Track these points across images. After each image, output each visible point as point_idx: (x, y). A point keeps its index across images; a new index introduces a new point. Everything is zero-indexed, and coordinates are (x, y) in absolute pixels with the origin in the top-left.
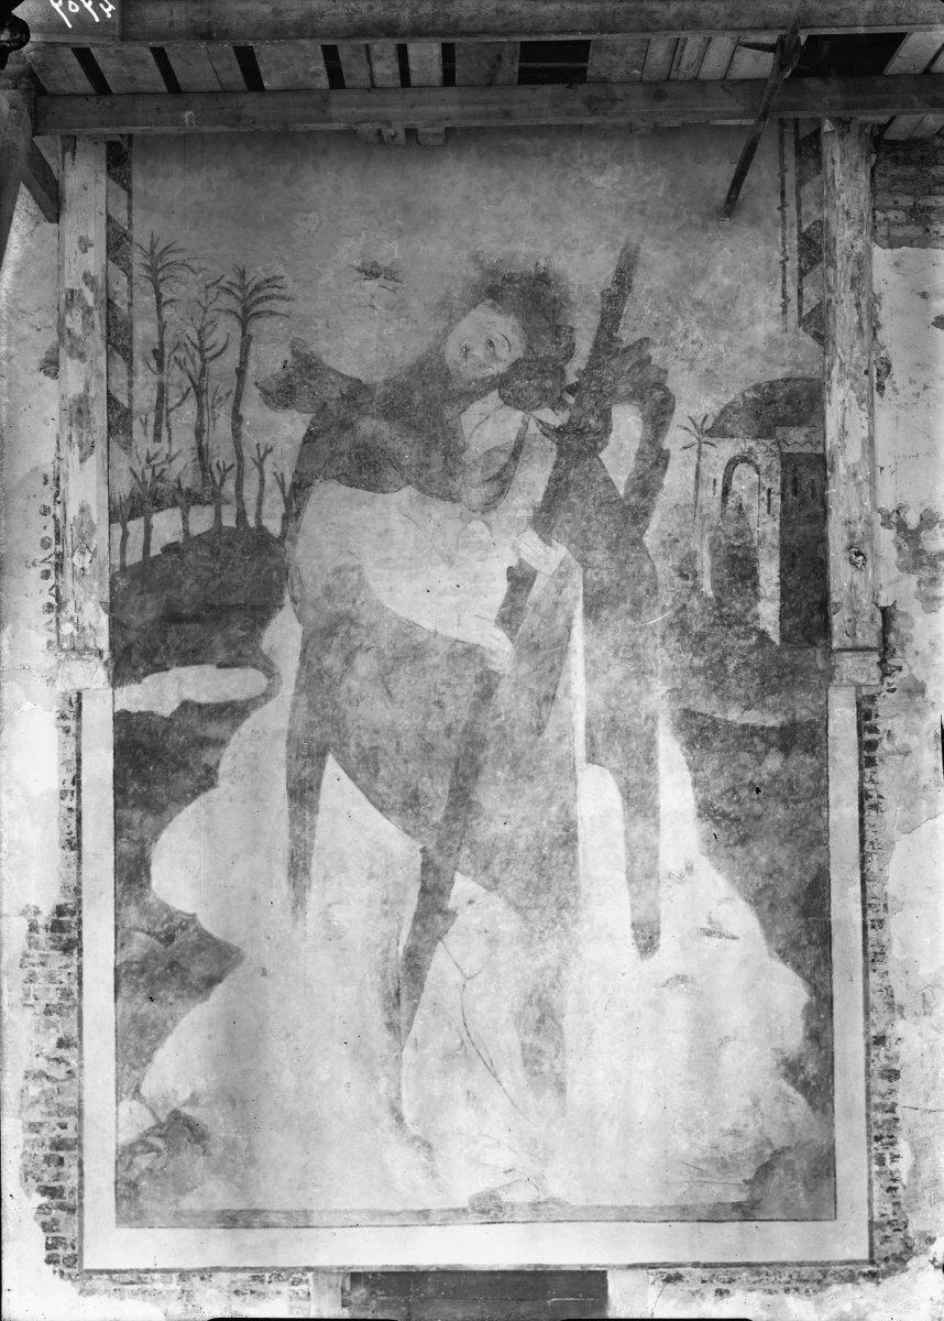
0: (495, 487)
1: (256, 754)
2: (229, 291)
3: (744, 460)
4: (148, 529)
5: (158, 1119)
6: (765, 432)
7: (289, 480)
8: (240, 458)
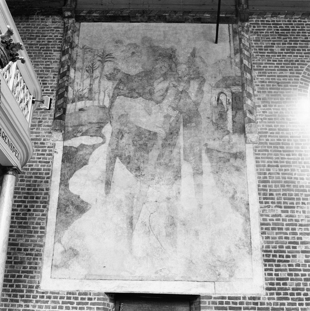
3: (222, 93)
4: (76, 105)
6: (227, 87)
7: (111, 95)
8: (100, 91)
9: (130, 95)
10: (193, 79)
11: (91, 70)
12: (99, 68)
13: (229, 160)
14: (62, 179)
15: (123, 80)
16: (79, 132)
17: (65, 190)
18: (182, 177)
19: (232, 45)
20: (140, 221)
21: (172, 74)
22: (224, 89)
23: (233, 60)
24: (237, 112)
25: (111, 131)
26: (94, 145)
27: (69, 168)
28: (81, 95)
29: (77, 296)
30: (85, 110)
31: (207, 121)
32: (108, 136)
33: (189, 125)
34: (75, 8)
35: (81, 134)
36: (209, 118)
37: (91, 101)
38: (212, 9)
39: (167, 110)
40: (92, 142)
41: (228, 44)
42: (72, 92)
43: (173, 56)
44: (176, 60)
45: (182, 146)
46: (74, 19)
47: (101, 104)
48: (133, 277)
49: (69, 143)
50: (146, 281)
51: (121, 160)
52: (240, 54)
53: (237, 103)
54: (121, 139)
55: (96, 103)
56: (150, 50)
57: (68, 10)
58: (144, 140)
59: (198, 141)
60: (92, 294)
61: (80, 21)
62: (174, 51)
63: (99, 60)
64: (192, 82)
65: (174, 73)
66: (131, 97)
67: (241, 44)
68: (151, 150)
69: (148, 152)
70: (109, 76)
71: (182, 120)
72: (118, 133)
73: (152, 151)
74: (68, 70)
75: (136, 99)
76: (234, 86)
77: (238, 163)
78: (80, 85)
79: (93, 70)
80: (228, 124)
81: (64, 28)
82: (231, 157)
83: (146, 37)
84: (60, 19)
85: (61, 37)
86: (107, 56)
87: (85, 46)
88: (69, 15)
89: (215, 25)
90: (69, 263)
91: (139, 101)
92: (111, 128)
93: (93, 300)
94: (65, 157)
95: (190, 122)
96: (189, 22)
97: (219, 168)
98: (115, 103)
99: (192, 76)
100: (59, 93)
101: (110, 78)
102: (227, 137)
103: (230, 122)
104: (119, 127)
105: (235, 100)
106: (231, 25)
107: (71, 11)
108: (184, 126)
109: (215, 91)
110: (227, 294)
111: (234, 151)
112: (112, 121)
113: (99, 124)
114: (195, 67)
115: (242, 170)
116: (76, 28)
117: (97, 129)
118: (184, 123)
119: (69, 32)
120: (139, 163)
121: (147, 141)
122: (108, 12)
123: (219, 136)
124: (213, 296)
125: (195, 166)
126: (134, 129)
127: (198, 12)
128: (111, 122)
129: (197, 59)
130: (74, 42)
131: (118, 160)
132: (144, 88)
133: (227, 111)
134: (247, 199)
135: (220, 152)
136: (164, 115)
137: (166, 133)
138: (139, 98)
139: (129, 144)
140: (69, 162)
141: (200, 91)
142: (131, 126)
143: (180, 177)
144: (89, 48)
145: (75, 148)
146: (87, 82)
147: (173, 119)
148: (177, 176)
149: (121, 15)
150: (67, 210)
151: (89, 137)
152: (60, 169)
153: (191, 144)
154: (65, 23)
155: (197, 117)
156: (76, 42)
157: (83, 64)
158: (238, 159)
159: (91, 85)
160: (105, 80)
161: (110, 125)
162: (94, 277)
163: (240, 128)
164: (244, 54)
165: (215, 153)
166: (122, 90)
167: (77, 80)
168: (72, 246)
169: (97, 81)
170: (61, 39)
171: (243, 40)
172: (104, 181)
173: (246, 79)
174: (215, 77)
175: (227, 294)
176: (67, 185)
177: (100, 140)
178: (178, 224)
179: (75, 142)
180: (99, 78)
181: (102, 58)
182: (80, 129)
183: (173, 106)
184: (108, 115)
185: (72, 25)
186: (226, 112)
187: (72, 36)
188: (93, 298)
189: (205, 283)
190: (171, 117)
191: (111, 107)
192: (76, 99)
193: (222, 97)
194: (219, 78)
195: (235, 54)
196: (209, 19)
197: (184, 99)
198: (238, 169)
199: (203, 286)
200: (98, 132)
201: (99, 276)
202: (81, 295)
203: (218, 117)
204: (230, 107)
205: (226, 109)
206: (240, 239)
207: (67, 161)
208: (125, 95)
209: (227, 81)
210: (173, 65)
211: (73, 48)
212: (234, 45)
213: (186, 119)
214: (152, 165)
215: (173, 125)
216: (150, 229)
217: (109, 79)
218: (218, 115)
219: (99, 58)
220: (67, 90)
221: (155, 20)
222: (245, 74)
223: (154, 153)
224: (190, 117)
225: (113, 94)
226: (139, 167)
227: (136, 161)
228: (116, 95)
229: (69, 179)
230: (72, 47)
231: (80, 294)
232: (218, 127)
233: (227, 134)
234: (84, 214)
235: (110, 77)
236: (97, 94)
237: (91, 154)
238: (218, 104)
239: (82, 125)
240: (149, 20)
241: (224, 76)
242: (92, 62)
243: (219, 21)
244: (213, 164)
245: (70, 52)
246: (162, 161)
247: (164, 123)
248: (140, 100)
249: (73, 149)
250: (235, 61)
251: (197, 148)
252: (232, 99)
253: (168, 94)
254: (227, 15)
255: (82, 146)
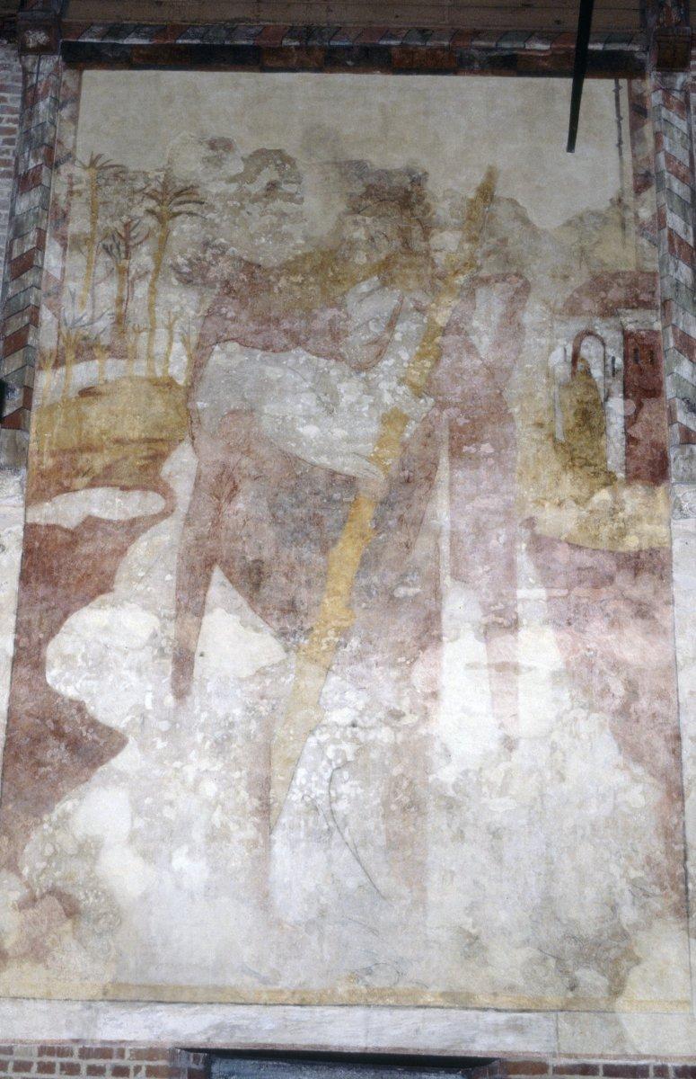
0: (374, 349)
1: (152, 562)
2: (151, 197)
3: (590, 333)
4: (67, 376)
5: (32, 892)
6: (608, 312)
7: (194, 339)
8: (153, 322)
9: (259, 340)
10: (485, 281)
11: (120, 245)
12: (151, 240)
13: (611, 579)
14: (21, 645)
15: (235, 285)
16: (80, 473)
17: (33, 683)
18: (444, 639)
19: (628, 156)
20: (296, 796)
21: (411, 265)
22: (598, 321)
23: (629, 215)
24: (640, 405)
25: (194, 472)
26: (133, 522)
27: (45, 604)
28: (85, 338)
29: (75, 1059)
30: (100, 394)
31: (535, 436)
32: (183, 489)
33: (472, 449)
34: (62, 14)
35: (86, 480)
36: (540, 425)
37: (123, 362)
38: (558, 22)
39: (393, 393)
40: (129, 509)
41: (615, 154)
42: (53, 327)
43: (414, 196)
44: (424, 213)
45: (447, 527)
46: (57, 58)
47: (159, 374)
48: (268, 992)
49: (45, 513)
50: (318, 1009)
51: (229, 575)
52: (658, 191)
53: (641, 371)
54: (230, 498)
55: (140, 368)
56: (332, 175)
57: (38, 26)
58: (313, 502)
59: (501, 510)
60: (127, 1055)
61: (81, 65)
62: (418, 180)
63: (150, 212)
64: (481, 293)
65: (420, 260)
66: (265, 348)
67: (661, 156)
68: (335, 541)
69: (325, 551)
70: (186, 269)
71: (446, 434)
72: (219, 478)
73: (340, 544)
74: (40, 246)
75: (282, 355)
76: (633, 308)
77: (642, 589)
78: (83, 303)
79: (128, 247)
80: (612, 447)
81: (24, 92)
82: (619, 567)
83: (319, 127)
84: (8, 56)
85: (11, 125)
86: (178, 194)
87: (99, 156)
88: (41, 41)
89: (564, 85)
90: (48, 943)
91: (291, 361)
92: (195, 461)
93: (132, 1074)
94: (31, 564)
95: (475, 440)
96: (472, 72)
97: (577, 606)
98: (208, 370)
99: (484, 273)
100: (9, 333)
101: (191, 277)
102: (604, 495)
103: (614, 440)
104: (220, 457)
105: (636, 361)
106: (623, 82)
107: (47, 29)
108: (455, 453)
109: (563, 328)
110: (601, 1056)
111: (632, 543)
112: (196, 433)
113: (153, 445)
114: (493, 240)
115: (657, 616)
116: (67, 89)
117: (143, 462)
118: (453, 443)
119: (42, 106)
120: (294, 586)
121: (321, 508)
122: (181, 31)
123: (576, 492)
124: (553, 1062)
125: (491, 600)
126: (273, 466)
127: (506, 33)
128: (193, 438)
129: (502, 211)
130: (60, 142)
131: (217, 575)
132: (309, 315)
133: (606, 400)
134: (675, 716)
135: (580, 547)
136: (381, 412)
137: (389, 478)
138: (293, 352)
139: (261, 520)
140: (47, 583)
141: (511, 325)
142: (263, 451)
143: (439, 638)
144: (112, 166)
145: (66, 531)
146: (108, 290)
147: (412, 427)
148: (429, 631)
149: (227, 43)
150: (39, 755)
151: (119, 492)
152: (13, 606)
153: (477, 520)
154: (26, 73)
155: (500, 420)
156: (69, 141)
157: (93, 223)
158: (645, 576)
159: (120, 301)
160: (170, 284)
161: (191, 448)
162: (133, 994)
163: (651, 463)
164: (670, 190)
165: (562, 555)
166: (234, 320)
167: (71, 285)
168: (59, 884)
169: (141, 290)
170: (12, 131)
171: (666, 140)
172: (168, 651)
173: (678, 284)
174: (566, 277)
175: (601, 1056)
176: (39, 666)
177: (155, 503)
178: (431, 807)
179: (68, 510)
180: (150, 277)
181: (160, 203)
182: (83, 460)
183: (415, 380)
184: (182, 410)
185: (53, 78)
186: (600, 405)
187: (53, 123)
188: (132, 1068)
189: (526, 1015)
190: (405, 419)
191: (191, 388)
192: (70, 356)
193: (590, 350)
194: (580, 279)
195: (639, 190)
196: (544, 59)
197: (455, 355)
198: (642, 611)
199: (518, 1029)
200: (145, 467)
201: (154, 988)
202: (88, 1057)
203: (572, 421)
204: (617, 386)
205: (603, 396)
206: (649, 860)
207: (37, 579)
208: (243, 342)
209: (606, 292)
210: (416, 232)
211: (57, 165)
212: (634, 156)
213: (461, 430)
214: (338, 593)
215: (415, 449)
216: (331, 824)
217: (187, 281)
218: (575, 414)
219: (151, 204)
220: (35, 321)
221: (349, 63)
222: (672, 265)
223: (347, 551)
224: (474, 421)
225: (201, 335)
226: (292, 603)
227: (284, 580)
228: (212, 340)
229: (47, 641)
230: (53, 164)
231: (85, 1053)
232: (572, 459)
233: (605, 485)
234: (100, 769)
235: (189, 274)
236: (144, 334)
237: (121, 552)
238: (573, 373)
239: (90, 448)
240: (331, 61)
241: (598, 271)
242: (125, 219)
243: (580, 66)
244: (555, 592)
245: (45, 182)
246: (375, 579)
247: (381, 441)
248: (297, 358)
249: (60, 536)
250: (637, 216)
251: (498, 536)
252: (626, 357)
253: (398, 337)
254: (611, 47)
255: (91, 524)
